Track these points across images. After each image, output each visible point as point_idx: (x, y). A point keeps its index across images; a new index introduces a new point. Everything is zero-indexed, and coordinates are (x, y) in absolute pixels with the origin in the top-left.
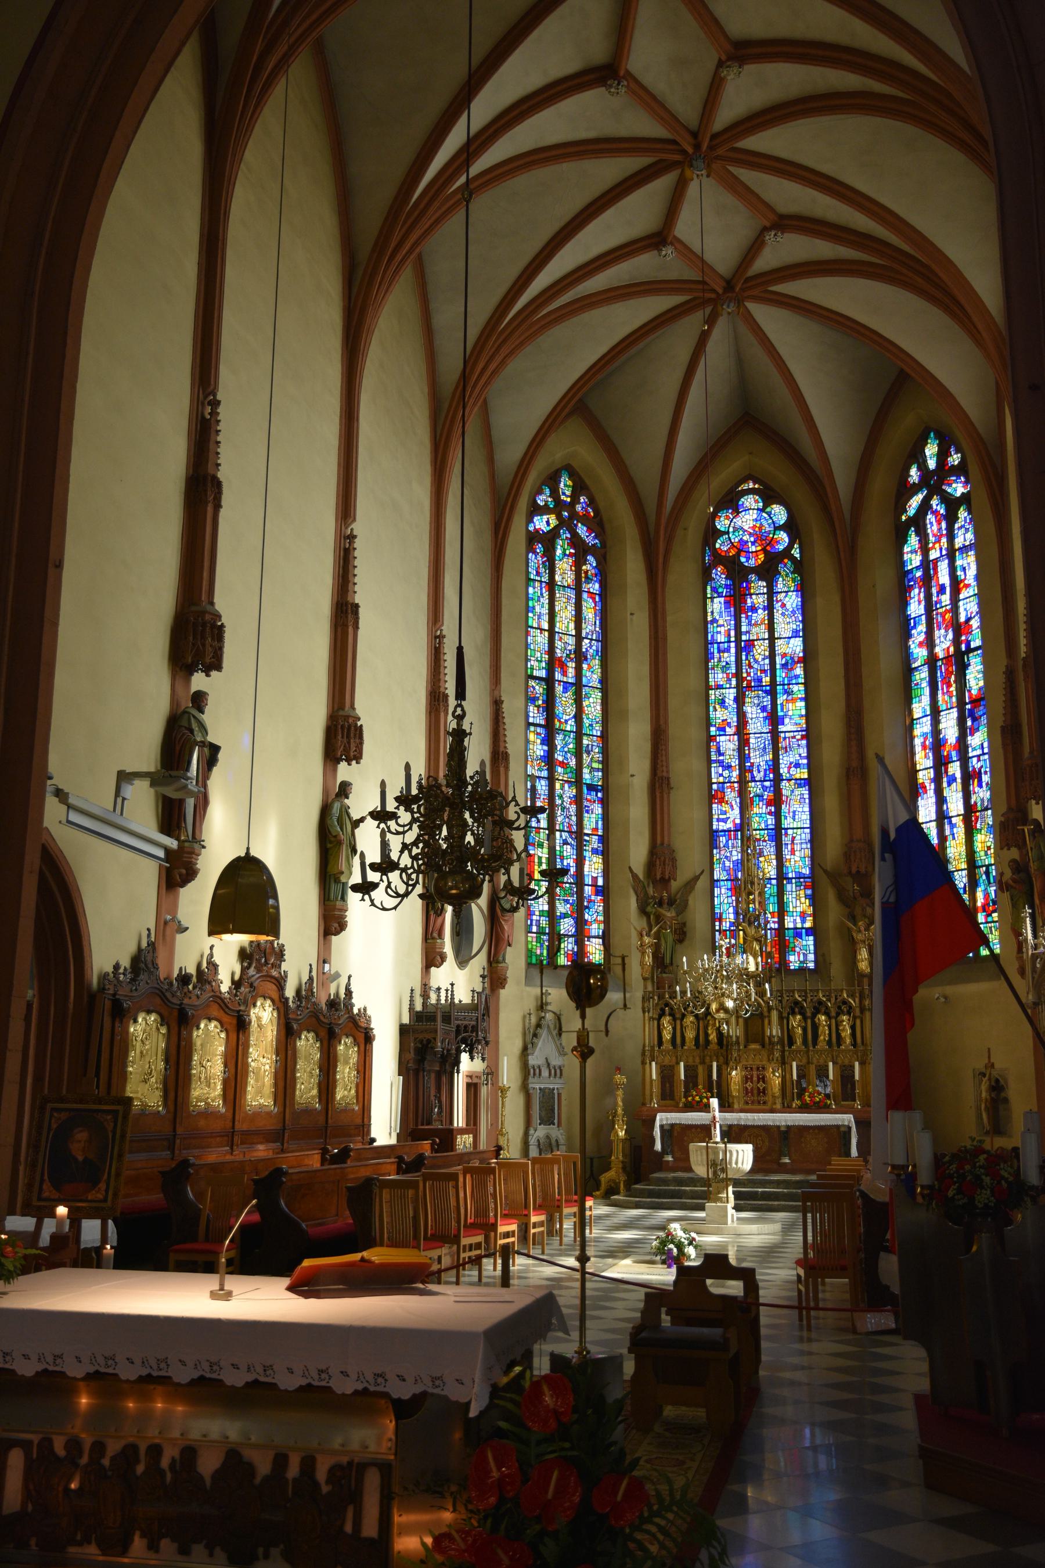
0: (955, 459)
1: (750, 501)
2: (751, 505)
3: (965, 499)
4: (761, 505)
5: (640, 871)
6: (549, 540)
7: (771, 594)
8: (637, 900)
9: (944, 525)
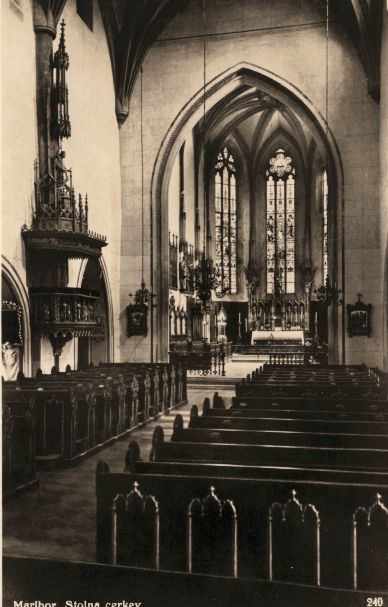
5: (246, 267)
6: (221, 171)
7: (285, 185)
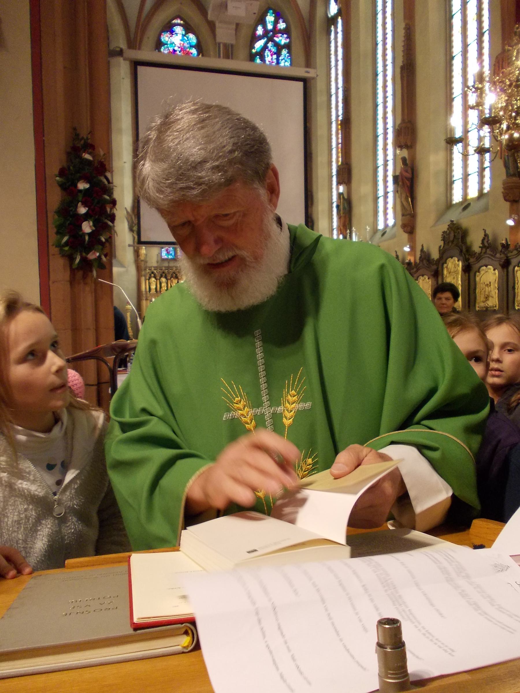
0: (282, 25)
1: (179, 30)
2: (179, 31)
3: (288, 46)
4: (184, 32)
5: (129, 210)
8: (128, 224)
9: (275, 57)
